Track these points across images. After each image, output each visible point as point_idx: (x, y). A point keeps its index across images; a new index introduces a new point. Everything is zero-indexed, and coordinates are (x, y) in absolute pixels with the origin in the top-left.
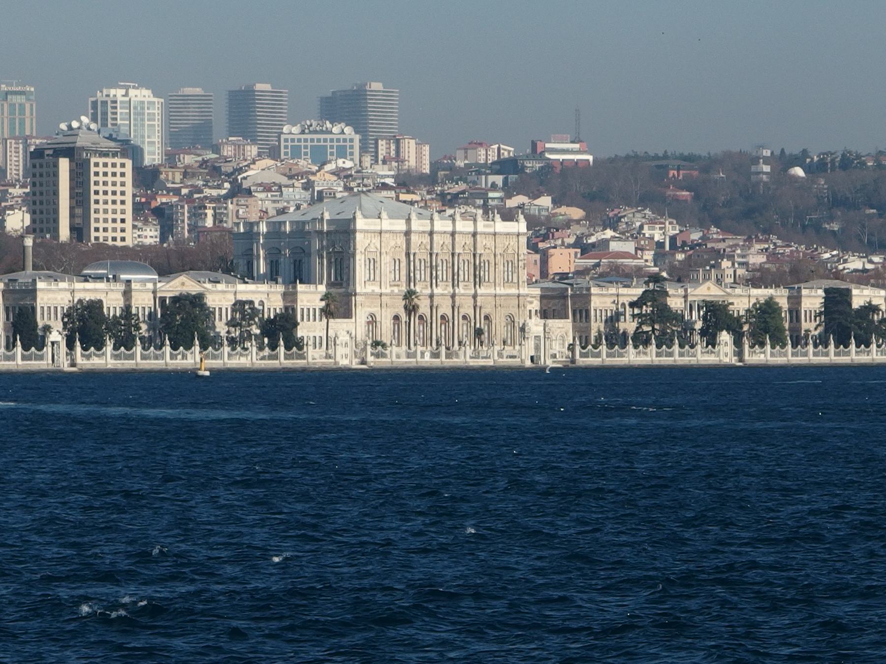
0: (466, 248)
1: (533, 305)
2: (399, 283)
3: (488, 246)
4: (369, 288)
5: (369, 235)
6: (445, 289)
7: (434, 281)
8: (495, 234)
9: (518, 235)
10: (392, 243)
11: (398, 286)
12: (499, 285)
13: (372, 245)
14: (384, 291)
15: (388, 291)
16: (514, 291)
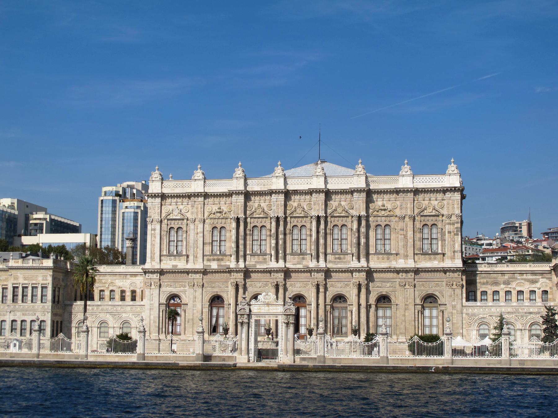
0: (339, 210)
1: (538, 285)
2: (220, 257)
3: (389, 206)
4: (167, 264)
5: (174, 200)
6: (300, 264)
7: (273, 253)
8: (397, 191)
9: (444, 191)
10: (215, 208)
11: (218, 260)
12: (406, 257)
13: (176, 212)
14: (190, 266)
15: (199, 266)
16: (435, 264)
